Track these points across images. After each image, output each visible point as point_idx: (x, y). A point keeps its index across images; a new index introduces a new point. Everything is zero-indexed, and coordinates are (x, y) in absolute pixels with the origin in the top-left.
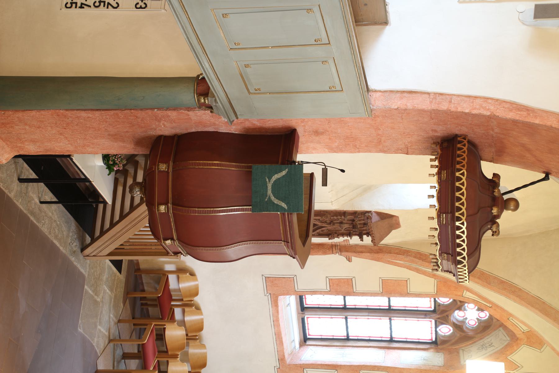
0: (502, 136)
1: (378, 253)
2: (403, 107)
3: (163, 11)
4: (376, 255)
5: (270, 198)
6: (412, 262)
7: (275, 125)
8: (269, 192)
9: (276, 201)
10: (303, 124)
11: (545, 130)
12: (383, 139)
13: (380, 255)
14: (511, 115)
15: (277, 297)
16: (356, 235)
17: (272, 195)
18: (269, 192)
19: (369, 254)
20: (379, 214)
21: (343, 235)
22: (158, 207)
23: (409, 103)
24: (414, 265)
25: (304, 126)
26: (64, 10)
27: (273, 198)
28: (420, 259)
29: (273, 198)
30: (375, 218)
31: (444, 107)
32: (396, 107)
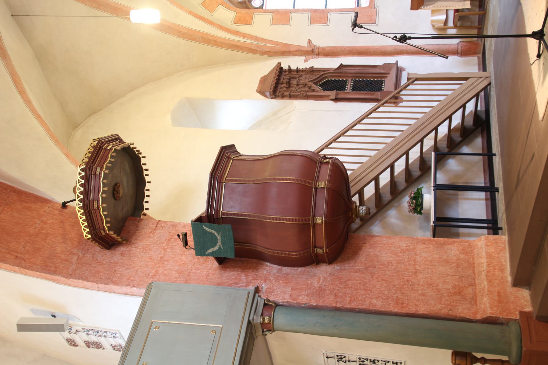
0: (75, 251)
1: (284, 52)
2: (128, 287)
3: (324, 352)
4: (286, 49)
5: (219, 234)
6: (259, 46)
7: (231, 273)
8: (219, 238)
9: (213, 231)
10: (210, 271)
11: (36, 264)
12: (164, 245)
13: (283, 49)
14: (56, 277)
15: (370, 5)
16: (294, 71)
17: (217, 236)
18: (219, 238)
19: (291, 50)
20: (266, 96)
21: (303, 71)
22: (322, 222)
23: (124, 289)
24: (258, 43)
25: (210, 269)
26: (403, 362)
27: (216, 234)
28: (253, 50)
29: (216, 234)
30: (268, 94)
31: (101, 286)
32: (133, 288)
